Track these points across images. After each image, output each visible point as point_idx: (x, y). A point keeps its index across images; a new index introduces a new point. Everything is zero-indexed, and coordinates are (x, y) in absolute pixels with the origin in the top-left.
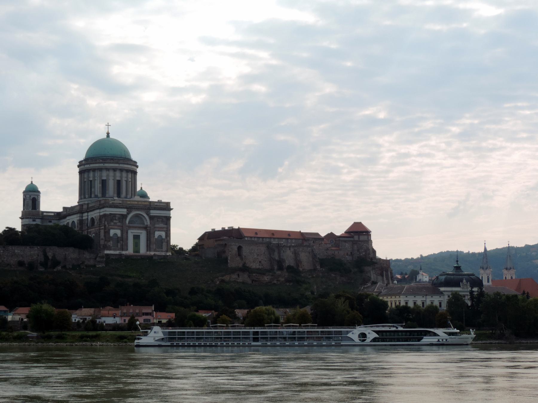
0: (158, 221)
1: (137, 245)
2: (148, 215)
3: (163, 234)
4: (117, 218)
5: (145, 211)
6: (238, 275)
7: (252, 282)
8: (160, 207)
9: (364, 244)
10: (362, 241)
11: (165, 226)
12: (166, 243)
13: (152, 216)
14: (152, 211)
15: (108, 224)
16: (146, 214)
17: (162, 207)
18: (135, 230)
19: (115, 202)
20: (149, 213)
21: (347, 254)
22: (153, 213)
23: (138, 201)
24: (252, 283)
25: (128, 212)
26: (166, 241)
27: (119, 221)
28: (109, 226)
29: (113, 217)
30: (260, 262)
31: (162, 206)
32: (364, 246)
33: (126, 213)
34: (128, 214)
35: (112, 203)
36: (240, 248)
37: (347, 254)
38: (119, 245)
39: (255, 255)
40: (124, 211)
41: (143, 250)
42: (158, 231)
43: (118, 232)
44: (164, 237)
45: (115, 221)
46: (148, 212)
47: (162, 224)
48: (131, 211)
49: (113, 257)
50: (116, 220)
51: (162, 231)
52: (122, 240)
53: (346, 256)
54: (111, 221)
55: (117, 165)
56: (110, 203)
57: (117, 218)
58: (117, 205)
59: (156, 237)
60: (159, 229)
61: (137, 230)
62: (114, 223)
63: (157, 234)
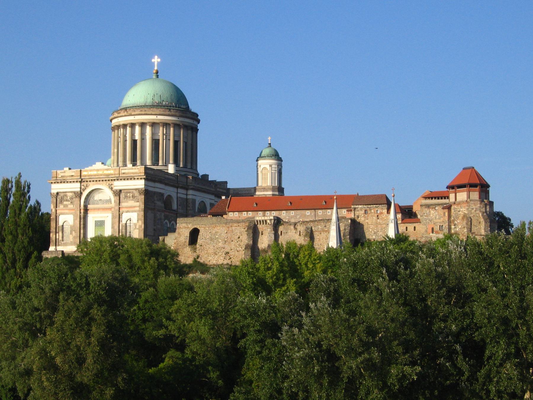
2: (112, 189)
5: (108, 184)
9: (461, 209)
10: (459, 203)
11: (138, 204)
12: (138, 230)
19: (66, 174)
20: (112, 186)
21: (433, 229)
22: (119, 185)
23: (98, 170)
27: (71, 203)
30: (227, 253)
31: (133, 173)
32: (460, 213)
34: (84, 190)
35: (62, 176)
37: (433, 229)
39: (219, 242)
40: (76, 187)
42: (127, 212)
45: (65, 203)
46: (112, 184)
47: (133, 201)
49: (47, 256)
50: (67, 200)
51: (132, 212)
52: (74, 231)
53: (431, 234)
54: (60, 203)
56: (59, 176)
58: (68, 178)
59: (124, 222)
62: (64, 206)
63: (125, 217)
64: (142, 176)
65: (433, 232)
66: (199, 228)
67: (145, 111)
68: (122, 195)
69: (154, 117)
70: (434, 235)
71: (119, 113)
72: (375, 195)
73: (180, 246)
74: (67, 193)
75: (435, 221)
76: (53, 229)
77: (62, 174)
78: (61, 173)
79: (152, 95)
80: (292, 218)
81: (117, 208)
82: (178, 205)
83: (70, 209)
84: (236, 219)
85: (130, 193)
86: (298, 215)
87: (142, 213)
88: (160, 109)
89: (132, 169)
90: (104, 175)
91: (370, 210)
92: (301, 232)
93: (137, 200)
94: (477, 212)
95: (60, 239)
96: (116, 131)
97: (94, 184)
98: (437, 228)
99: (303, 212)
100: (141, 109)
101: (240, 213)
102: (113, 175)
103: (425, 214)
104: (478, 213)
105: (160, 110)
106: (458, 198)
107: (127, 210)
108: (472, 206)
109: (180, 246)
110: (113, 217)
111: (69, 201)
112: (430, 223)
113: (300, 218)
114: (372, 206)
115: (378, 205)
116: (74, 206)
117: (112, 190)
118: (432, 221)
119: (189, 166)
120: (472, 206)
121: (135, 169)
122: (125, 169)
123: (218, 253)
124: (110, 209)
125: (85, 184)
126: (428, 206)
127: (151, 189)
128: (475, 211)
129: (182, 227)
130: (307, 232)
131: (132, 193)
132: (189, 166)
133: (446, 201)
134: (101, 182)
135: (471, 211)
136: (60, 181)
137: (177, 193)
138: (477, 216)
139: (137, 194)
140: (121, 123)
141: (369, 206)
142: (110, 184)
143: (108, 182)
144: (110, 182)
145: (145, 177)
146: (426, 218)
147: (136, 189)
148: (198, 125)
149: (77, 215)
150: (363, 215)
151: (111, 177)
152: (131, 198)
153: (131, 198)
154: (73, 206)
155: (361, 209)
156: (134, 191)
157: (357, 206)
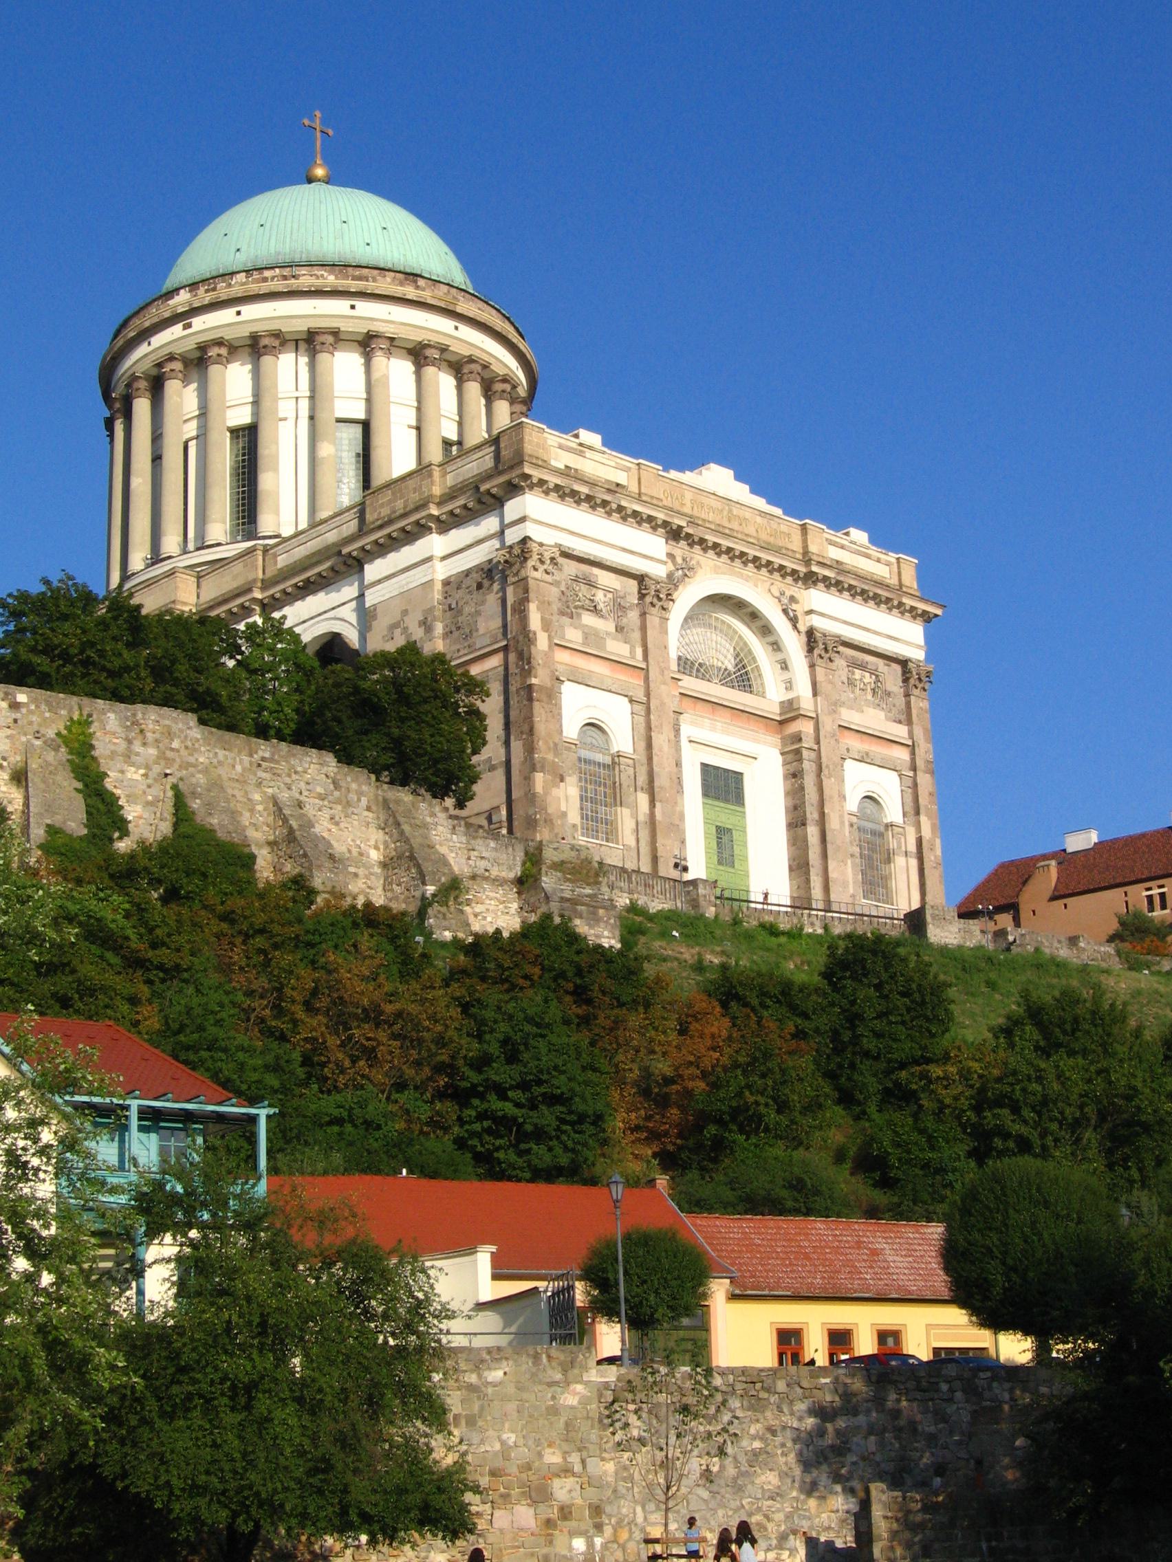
0: (851, 683)
4: (600, 596)
14: (816, 598)
15: (546, 626)
16: (785, 611)
18: (713, 729)
20: (794, 606)
29: (576, 579)
45: (588, 619)
47: (882, 715)
55: (443, 325)
62: (586, 636)
74: (596, 571)
78: (561, 447)
85: (863, 667)
97: (716, 570)
116: (632, 652)
117: (795, 627)
121: (879, 561)
122: (842, 547)
139: (892, 677)
142: (788, 594)
154: (627, 647)
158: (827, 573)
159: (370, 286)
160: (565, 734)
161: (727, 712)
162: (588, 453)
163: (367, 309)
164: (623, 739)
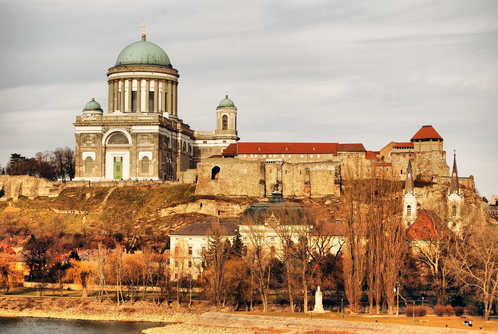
0: (143, 139)
1: (118, 168)
2: (130, 132)
3: (149, 155)
5: (126, 128)
6: (201, 205)
7: (219, 212)
8: (146, 121)
11: (153, 145)
13: (134, 133)
14: (134, 128)
16: (128, 131)
17: (147, 121)
18: (117, 151)
19: (89, 119)
20: (130, 130)
21: (402, 171)
22: (136, 129)
24: (219, 214)
25: (104, 130)
26: (153, 163)
28: (80, 148)
29: (86, 136)
31: (148, 120)
33: (101, 132)
34: (105, 132)
36: (216, 170)
37: (402, 171)
38: (94, 170)
40: (99, 129)
41: (126, 175)
43: (93, 155)
44: (150, 158)
45: (88, 142)
46: (130, 128)
48: (108, 129)
50: (89, 140)
53: (400, 175)
54: (83, 142)
56: (82, 120)
57: (91, 138)
58: (91, 122)
60: (144, 149)
61: (119, 151)
62: (87, 145)
63: (141, 155)
64: (157, 123)
65: (401, 173)
66: (219, 167)
67: (143, 68)
68: (139, 137)
69: (150, 74)
70: (403, 175)
71: (119, 69)
72: (354, 144)
73: (205, 180)
75: (403, 165)
76: (77, 163)
77: (86, 119)
79: (147, 55)
80: (289, 160)
81: (135, 147)
82: (172, 145)
83: (92, 148)
84: (245, 159)
85: (145, 136)
86: (294, 157)
87: (157, 152)
88: (155, 67)
89: (148, 117)
90: (123, 121)
91: (352, 155)
92: (302, 171)
93: (152, 141)
94: (437, 159)
95: (84, 171)
96: (116, 84)
97: (114, 128)
98: (405, 170)
99: (298, 155)
100: (140, 67)
101: (248, 155)
102: (131, 121)
103: (396, 160)
104: (438, 160)
105: (155, 68)
106: (421, 148)
107: (144, 149)
108: (434, 155)
109: (205, 180)
110: (131, 155)
111: (91, 141)
112: (399, 167)
113: (295, 160)
114: (354, 152)
115: (358, 152)
116: (96, 145)
118: (401, 165)
119: (174, 114)
120: (434, 155)
121: (150, 117)
123: (236, 185)
124: (128, 148)
125: (106, 127)
126: (398, 154)
127: (162, 133)
128: (436, 158)
129: (205, 165)
130: (307, 171)
131: (148, 136)
132: (174, 114)
133: (412, 150)
134: (120, 126)
135: (433, 158)
136: (84, 124)
137: (172, 135)
138: (438, 163)
139: (151, 137)
140: (122, 77)
141: (351, 152)
142: (128, 128)
143: (127, 127)
144: (128, 127)
145: (160, 124)
146: (396, 162)
147: (151, 133)
148: (178, 79)
149: (99, 152)
150: (346, 159)
151: (130, 123)
152: (147, 140)
153: (147, 140)
155: (345, 154)
156: (149, 135)
157: (342, 152)
158: (133, 124)
159: (120, 71)
160: (83, 159)
161: (120, 148)
162: (89, 117)
163: (120, 74)
164: (94, 158)
